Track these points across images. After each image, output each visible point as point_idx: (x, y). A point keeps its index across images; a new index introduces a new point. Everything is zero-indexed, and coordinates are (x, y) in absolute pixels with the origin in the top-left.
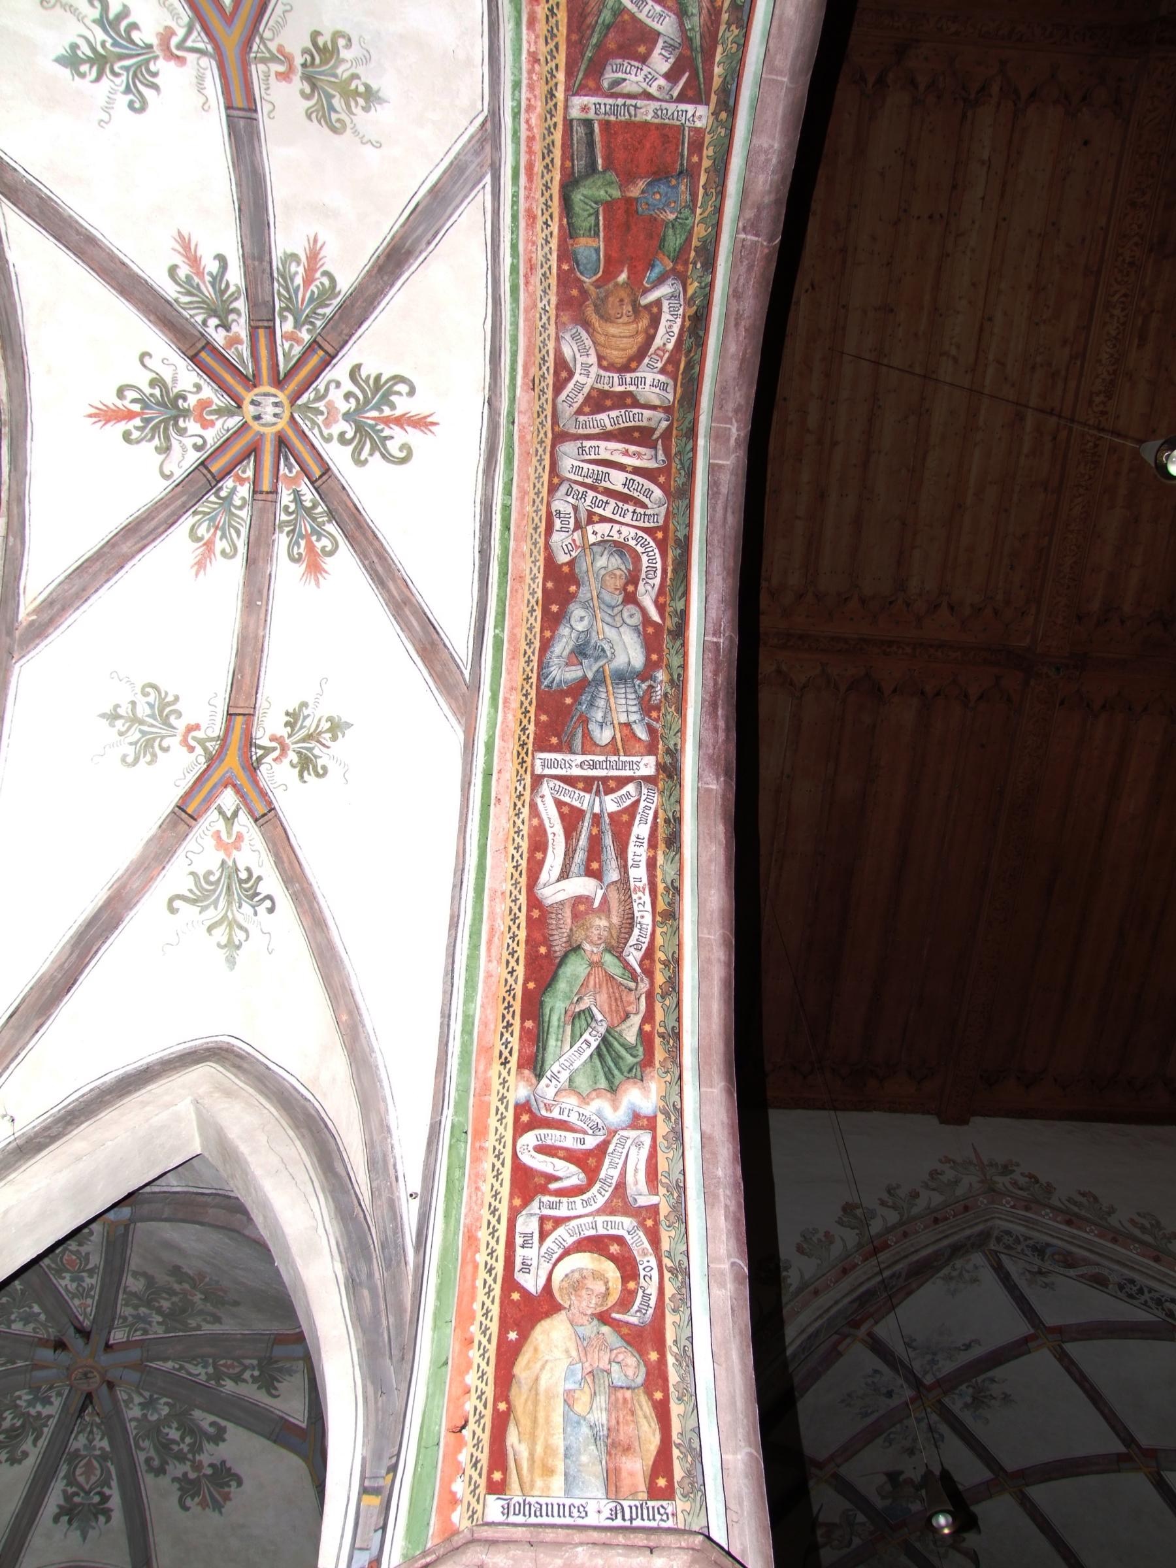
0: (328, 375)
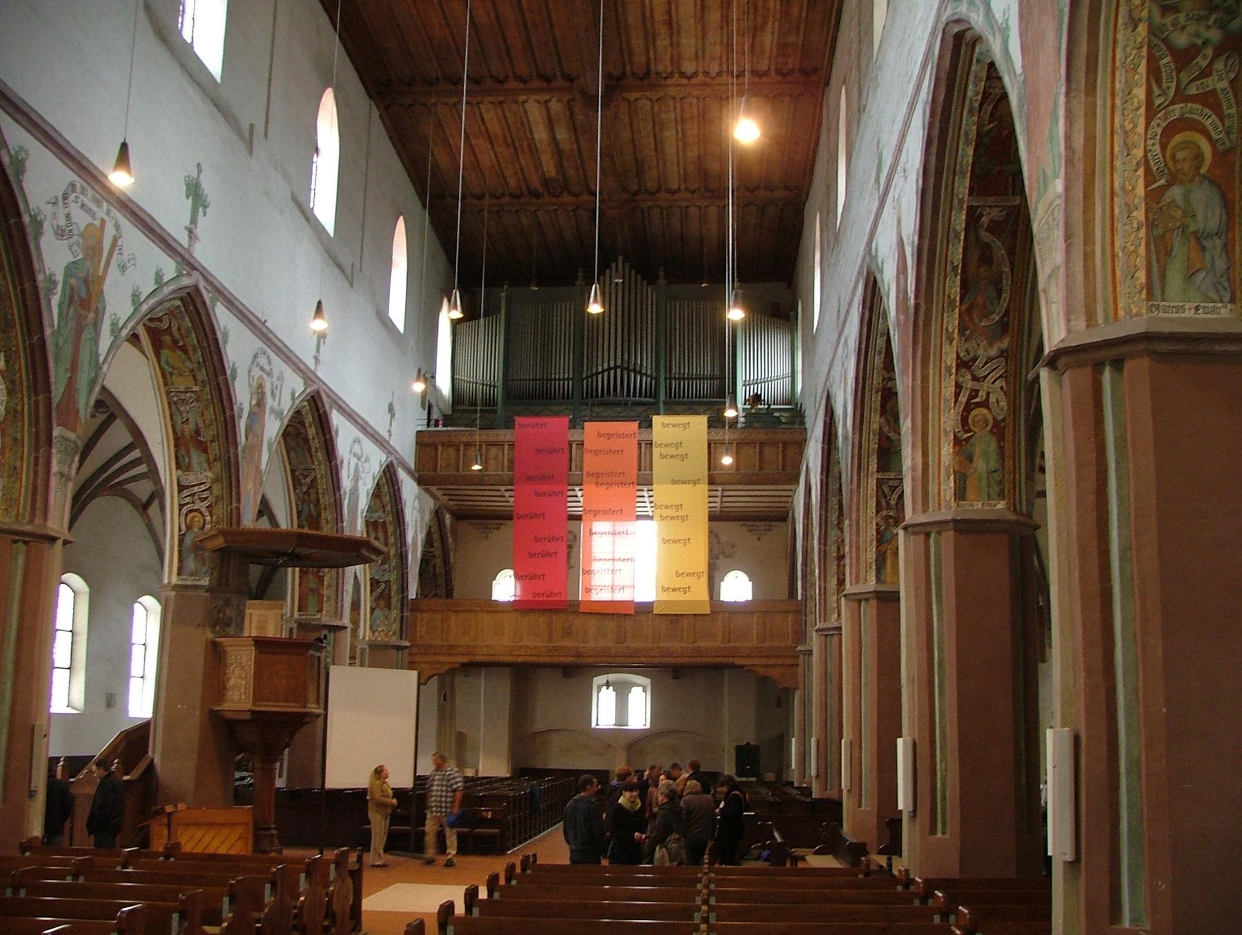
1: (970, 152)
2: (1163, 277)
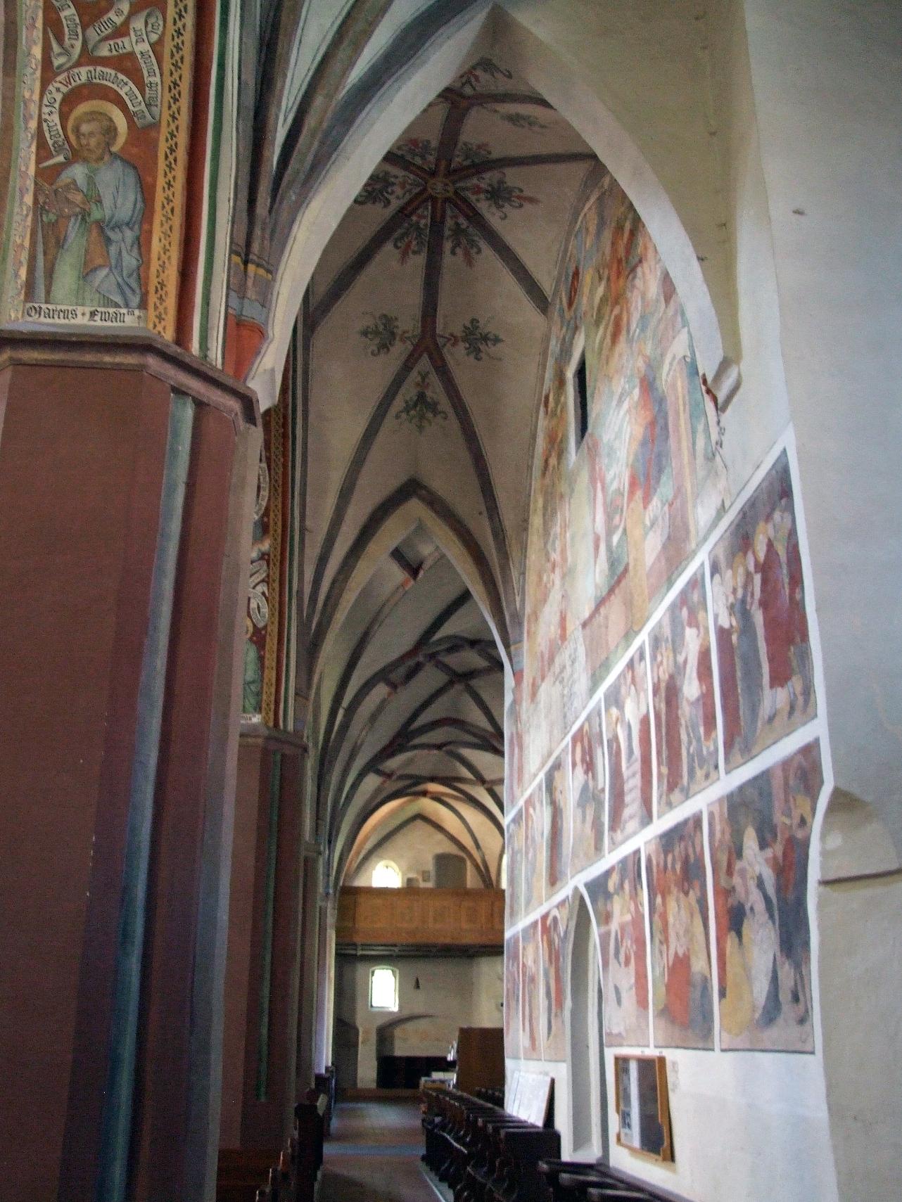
0: (401, 202)
2: (50, 274)
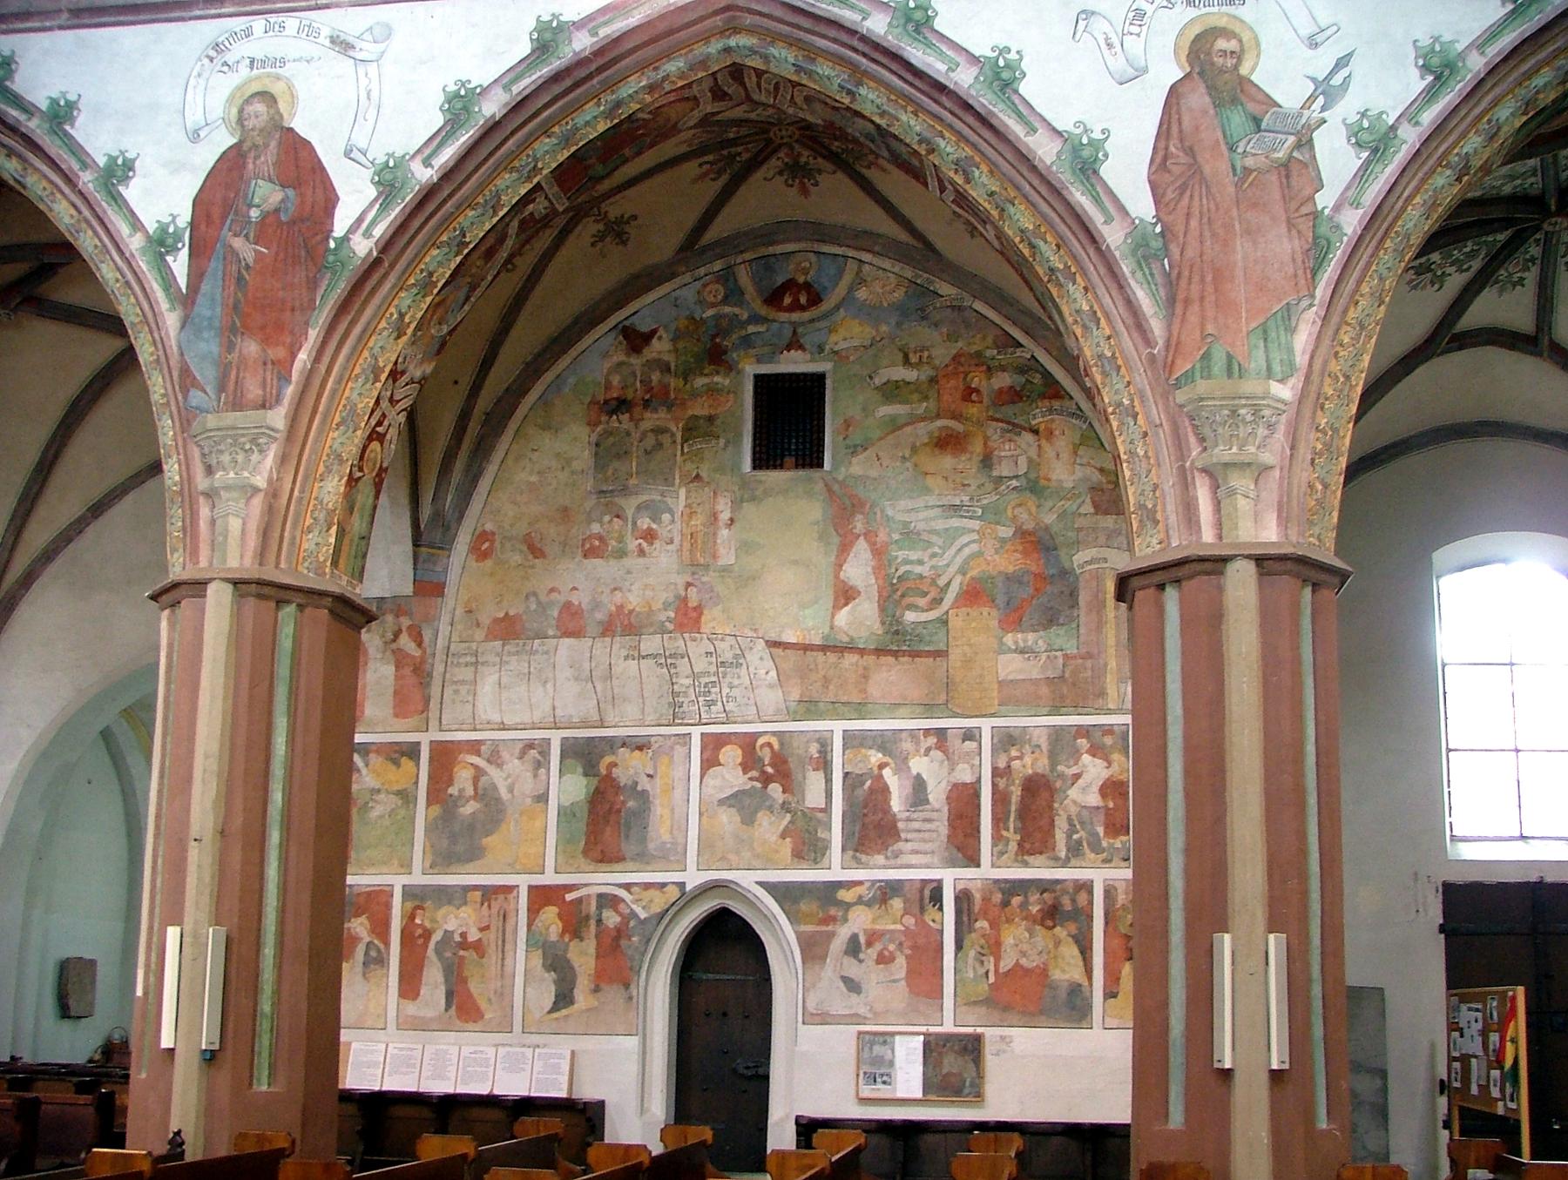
1: (602, 127)
